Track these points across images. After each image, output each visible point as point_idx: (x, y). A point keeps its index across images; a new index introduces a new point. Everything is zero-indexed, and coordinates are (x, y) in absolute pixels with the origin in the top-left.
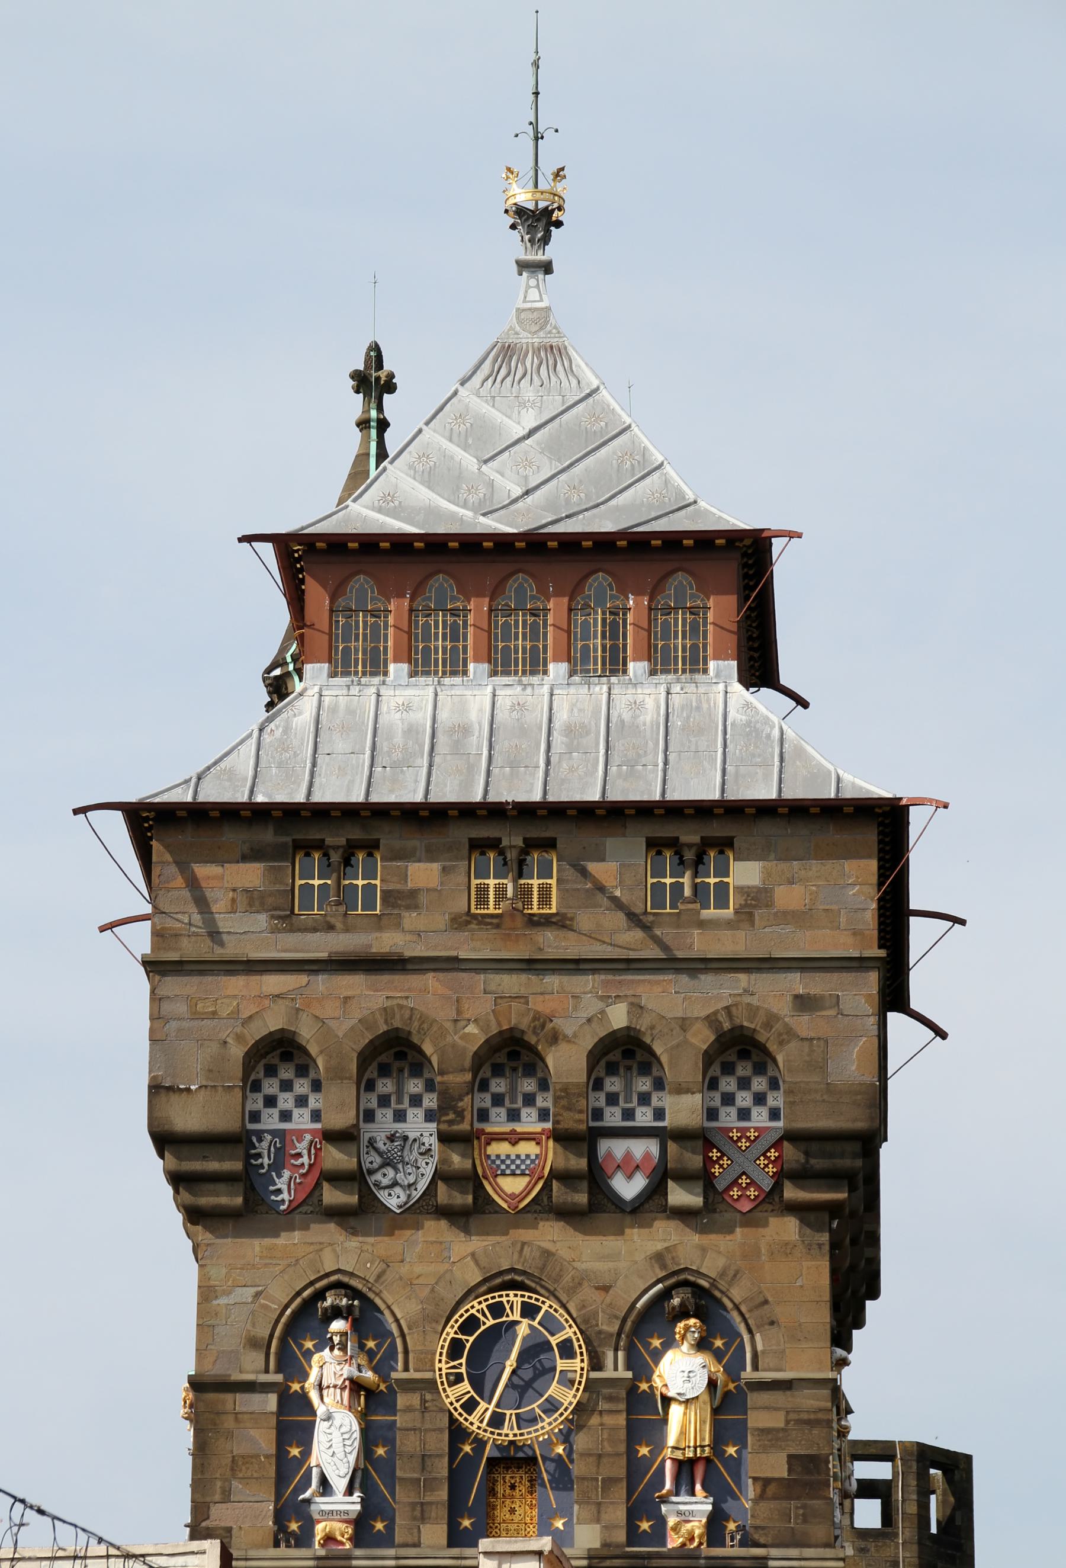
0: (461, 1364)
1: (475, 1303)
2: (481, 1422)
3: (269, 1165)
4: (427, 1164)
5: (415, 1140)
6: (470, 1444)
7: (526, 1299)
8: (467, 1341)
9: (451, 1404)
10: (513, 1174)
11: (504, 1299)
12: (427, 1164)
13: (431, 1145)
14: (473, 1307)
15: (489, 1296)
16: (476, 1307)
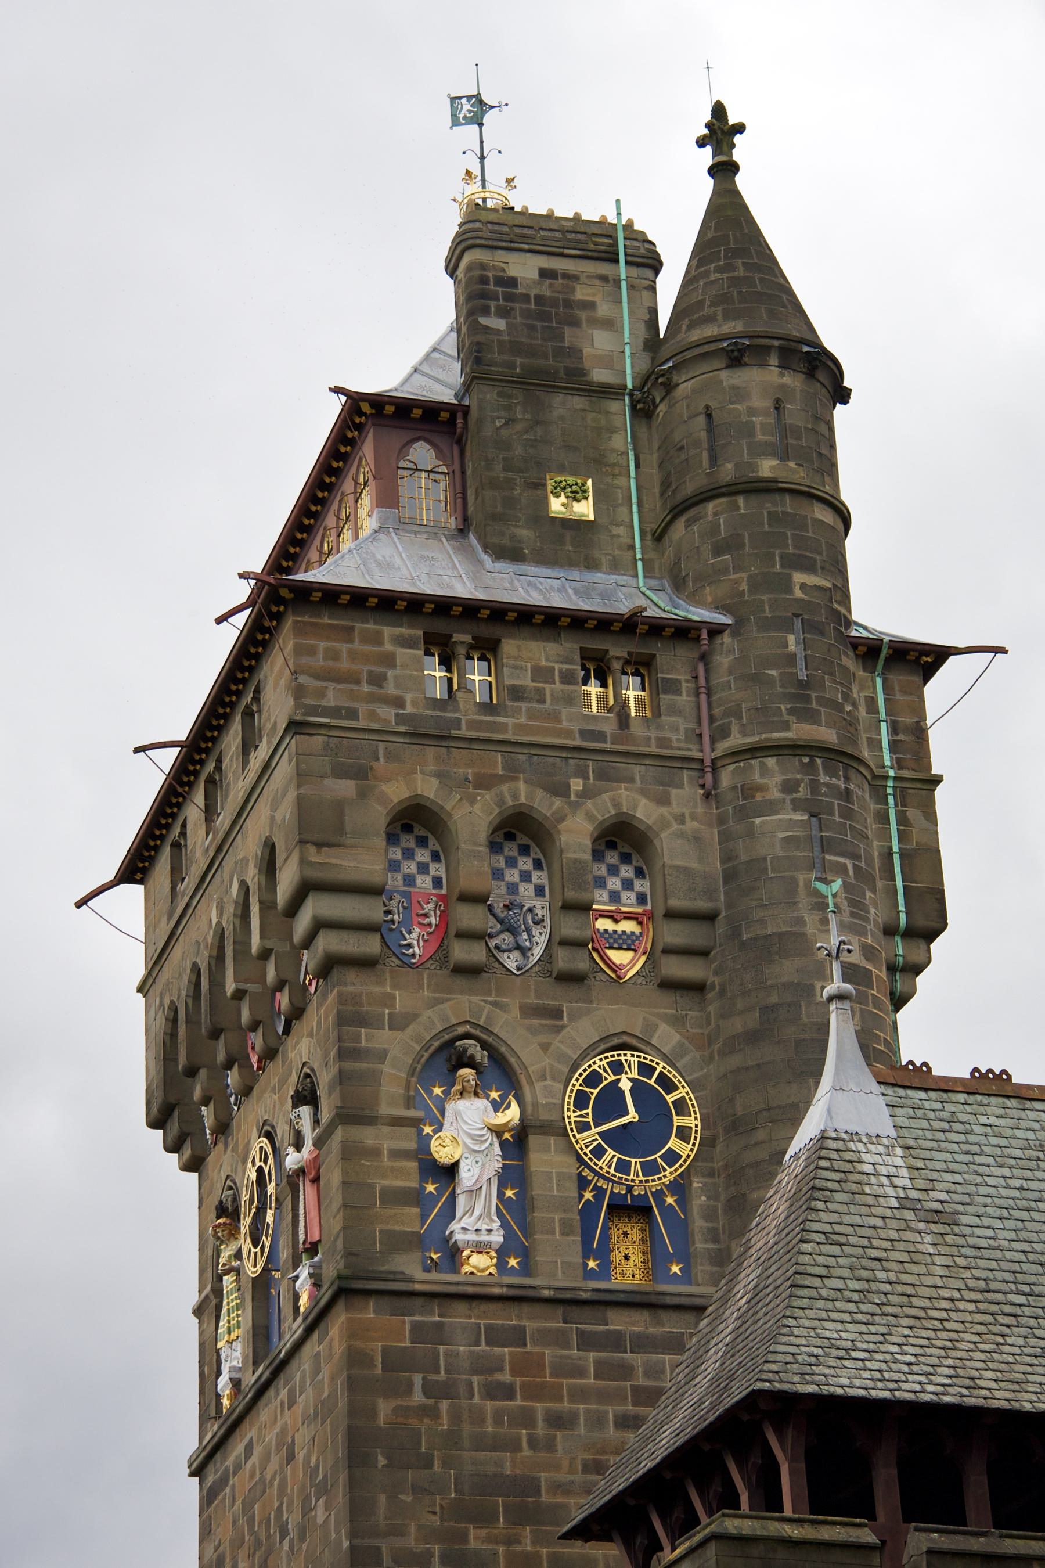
0: (587, 1114)
1: (596, 1059)
2: (610, 1167)
3: (399, 922)
4: (541, 933)
5: (530, 910)
6: (591, 1192)
7: (641, 1060)
8: (592, 1093)
9: (581, 1149)
10: (620, 948)
11: (623, 1058)
12: (541, 933)
13: (543, 916)
14: (594, 1063)
15: (609, 1054)
16: (599, 1063)
